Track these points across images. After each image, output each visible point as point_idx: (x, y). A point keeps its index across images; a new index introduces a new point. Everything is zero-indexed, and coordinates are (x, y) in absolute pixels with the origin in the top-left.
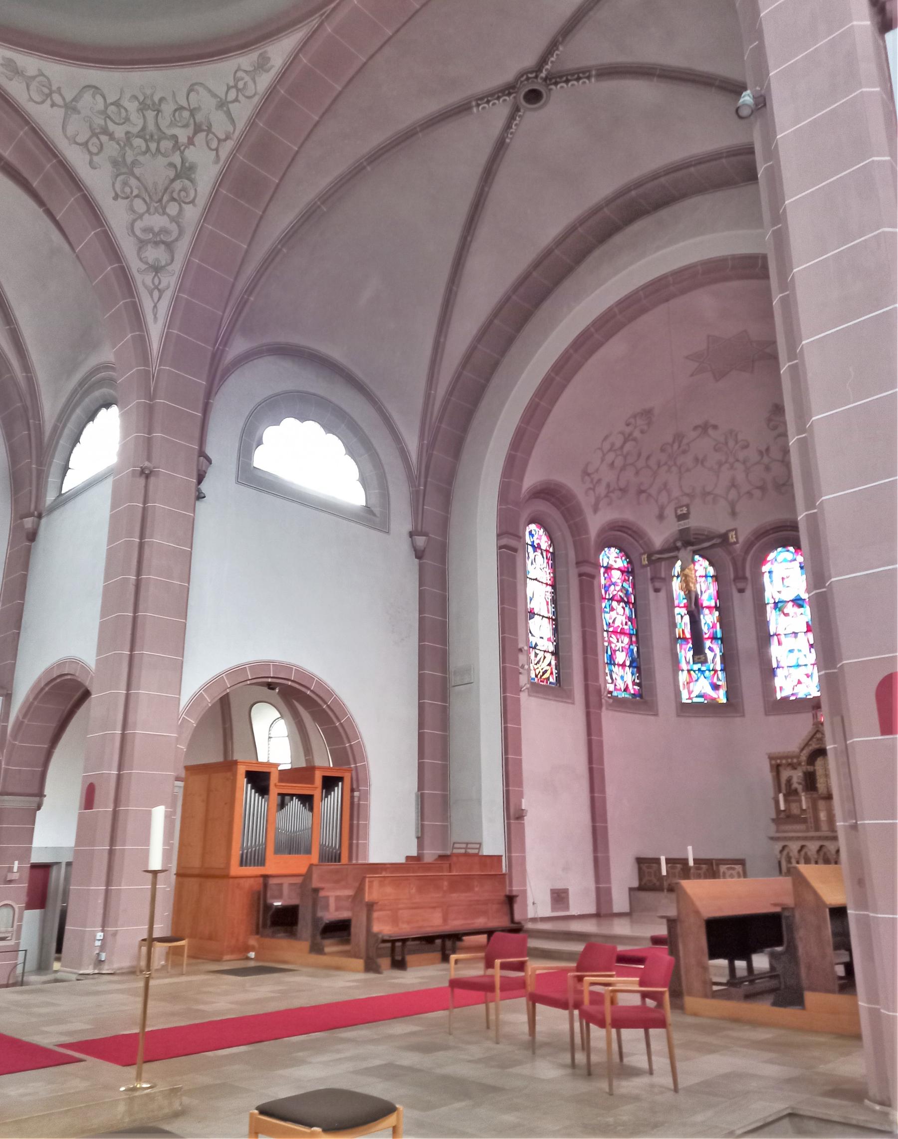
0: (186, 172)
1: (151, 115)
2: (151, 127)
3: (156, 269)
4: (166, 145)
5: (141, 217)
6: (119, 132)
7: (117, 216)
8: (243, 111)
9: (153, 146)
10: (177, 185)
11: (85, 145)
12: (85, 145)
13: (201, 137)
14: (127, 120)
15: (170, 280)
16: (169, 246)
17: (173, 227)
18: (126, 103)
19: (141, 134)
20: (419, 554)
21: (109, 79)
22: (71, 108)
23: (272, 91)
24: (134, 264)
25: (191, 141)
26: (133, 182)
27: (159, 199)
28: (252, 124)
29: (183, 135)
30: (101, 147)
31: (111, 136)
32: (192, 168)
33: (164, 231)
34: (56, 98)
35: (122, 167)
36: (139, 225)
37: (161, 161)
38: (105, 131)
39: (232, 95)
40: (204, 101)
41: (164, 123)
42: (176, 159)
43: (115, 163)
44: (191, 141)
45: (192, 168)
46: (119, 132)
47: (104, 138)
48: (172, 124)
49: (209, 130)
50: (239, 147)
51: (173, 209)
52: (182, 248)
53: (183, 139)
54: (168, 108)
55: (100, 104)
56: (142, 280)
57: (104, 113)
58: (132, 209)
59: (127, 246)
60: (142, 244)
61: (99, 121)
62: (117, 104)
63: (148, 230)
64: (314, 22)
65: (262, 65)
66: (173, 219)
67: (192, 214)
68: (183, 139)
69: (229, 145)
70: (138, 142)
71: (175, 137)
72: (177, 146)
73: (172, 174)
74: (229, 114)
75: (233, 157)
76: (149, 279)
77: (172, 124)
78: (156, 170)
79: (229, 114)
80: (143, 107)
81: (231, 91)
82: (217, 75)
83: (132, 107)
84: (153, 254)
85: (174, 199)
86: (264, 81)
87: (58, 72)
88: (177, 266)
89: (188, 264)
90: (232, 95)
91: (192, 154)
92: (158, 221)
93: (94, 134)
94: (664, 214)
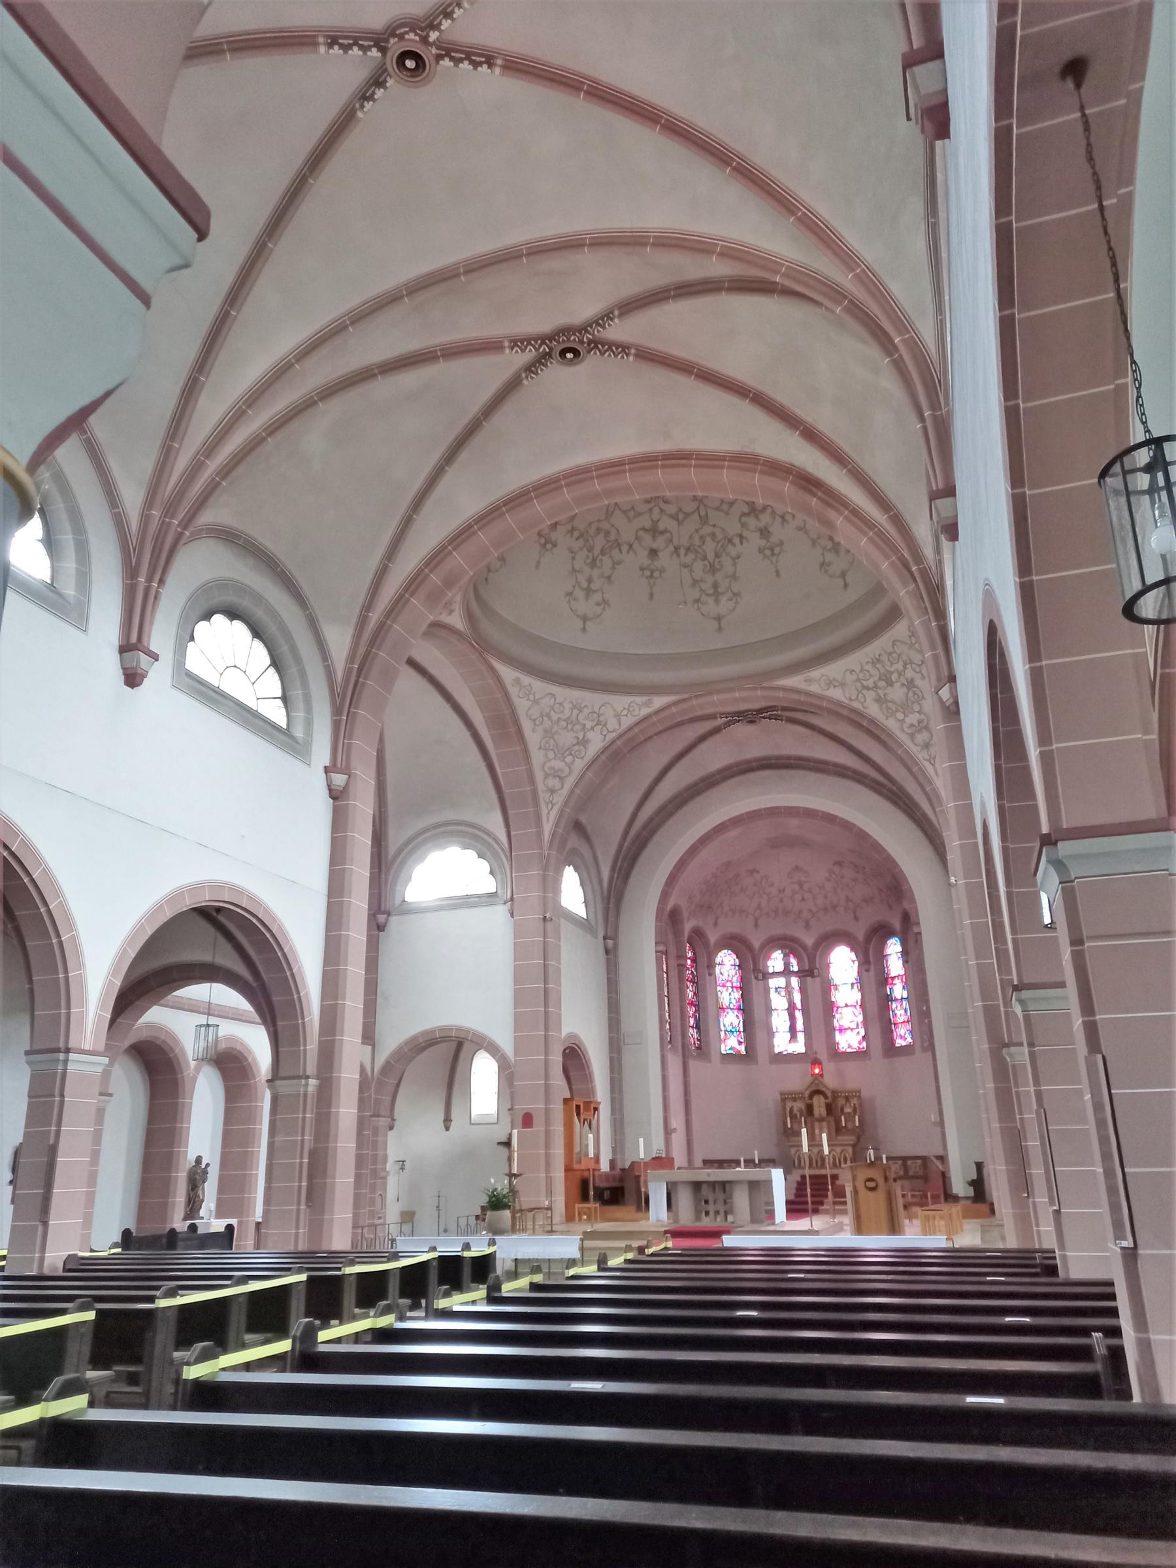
0: (584, 742)
1: (575, 712)
3: (552, 791)
4: (578, 727)
6: (555, 717)
7: (537, 758)
8: (627, 722)
9: (570, 727)
10: (576, 748)
11: (534, 720)
15: (559, 799)
16: (562, 779)
17: (567, 770)
18: (566, 705)
20: (607, 952)
21: (560, 692)
25: (592, 728)
26: (552, 742)
28: (630, 729)
29: (589, 725)
32: (588, 741)
33: (562, 771)
35: (549, 733)
37: (572, 734)
38: (548, 716)
39: (625, 712)
40: (608, 713)
41: (580, 717)
43: (546, 731)
44: (592, 728)
45: (588, 741)
46: (555, 717)
48: (587, 718)
49: (605, 725)
50: (620, 736)
51: (569, 759)
52: (570, 782)
53: (588, 726)
54: (586, 711)
56: (543, 796)
57: (552, 708)
58: (546, 756)
59: (539, 776)
60: (547, 776)
61: (547, 710)
62: (560, 704)
63: (551, 768)
66: (569, 766)
67: (579, 765)
68: (588, 726)
69: (614, 734)
70: (564, 724)
73: (575, 741)
75: (613, 742)
77: (587, 718)
78: (566, 738)
80: (574, 707)
82: (620, 702)
83: (567, 706)
84: (553, 782)
87: (538, 686)
89: (572, 791)
90: (625, 712)
91: (590, 735)
93: (542, 716)
94: (784, 772)
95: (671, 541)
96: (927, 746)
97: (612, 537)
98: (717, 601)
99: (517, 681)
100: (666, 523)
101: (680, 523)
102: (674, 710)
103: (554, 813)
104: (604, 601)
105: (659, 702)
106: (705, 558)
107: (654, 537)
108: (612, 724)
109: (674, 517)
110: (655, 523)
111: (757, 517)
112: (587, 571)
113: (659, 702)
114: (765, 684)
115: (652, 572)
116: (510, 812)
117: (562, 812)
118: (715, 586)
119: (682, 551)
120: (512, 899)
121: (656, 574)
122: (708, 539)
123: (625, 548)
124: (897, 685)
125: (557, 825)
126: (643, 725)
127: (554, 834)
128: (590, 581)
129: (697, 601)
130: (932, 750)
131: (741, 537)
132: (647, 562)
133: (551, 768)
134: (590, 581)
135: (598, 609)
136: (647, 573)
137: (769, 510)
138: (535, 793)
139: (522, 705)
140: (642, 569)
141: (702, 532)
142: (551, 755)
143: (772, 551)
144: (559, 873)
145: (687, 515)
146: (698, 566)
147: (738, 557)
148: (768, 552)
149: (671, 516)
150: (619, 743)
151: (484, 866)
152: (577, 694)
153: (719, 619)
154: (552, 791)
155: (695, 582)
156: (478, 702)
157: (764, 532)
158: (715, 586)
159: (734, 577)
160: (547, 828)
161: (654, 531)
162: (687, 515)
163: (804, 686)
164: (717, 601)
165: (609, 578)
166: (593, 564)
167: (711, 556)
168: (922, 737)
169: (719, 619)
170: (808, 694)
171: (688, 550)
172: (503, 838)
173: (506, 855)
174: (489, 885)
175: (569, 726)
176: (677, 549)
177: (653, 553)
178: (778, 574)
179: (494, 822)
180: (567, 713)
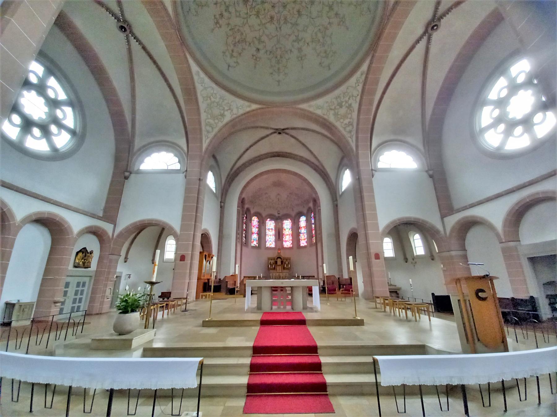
0: (223, 115)
1: (221, 100)
2: (220, 103)
3: (208, 132)
4: (221, 108)
5: (208, 119)
6: (213, 99)
7: (203, 116)
8: (241, 112)
12: (204, 97)
13: (229, 111)
14: (216, 98)
15: (211, 135)
16: (212, 128)
19: (217, 103)
22: (205, 88)
23: (248, 112)
24: (203, 128)
25: (227, 110)
26: (210, 111)
27: (214, 117)
28: (242, 115)
29: (226, 108)
30: (207, 100)
31: (210, 99)
34: (203, 85)
36: (207, 120)
42: (222, 112)
43: (208, 105)
44: (227, 110)
45: (225, 115)
47: (209, 99)
50: (236, 118)
51: (216, 121)
52: (216, 130)
54: (226, 102)
55: (212, 92)
56: (204, 133)
59: (203, 124)
60: (207, 125)
62: (215, 94)
64: (264, 106)
65: (249, 106)
67: (220, 125)
69: (235, 116)
70: (216, 104)
71: (224, 108)
72: (224, 109)
74: (238, 110)
76: (206, 133)
78: (216, 112)
79: (238, 110)
80: (220, 98)
81: (241, 107)
82: (240, 102)
83: (218, 96)
84: (209, 128)
85: (217, 119)
86: (248, 109)
87: (207, 80)
88: (214, 133)
91: (226, 113)
92: (211, 121)
93: (207, 97)
95: (265, 46)
96: (350, 132)
97: (243, 37)
98: (279, 76)
99: (198, 73)
100: (264, 38)
101: (270, 39)
102: (259, 111)
103: (208, 141)
104: (237, 62)
105: (254, 106)
106: (276, 57)
107: (259, 43)
108: (235, 111)
109: (267, 36)
110: (261, 36)
111: (298, 43)
112: (232, 47)
113: (254, 106)
114: (294, 106)
115: (256, 58)
116: (190, 136)
117: (211, 141)
118: (279, 69)
119: (268, 53)
120: (186, 171)
121: (258, 59)
122: (279, 50)
123: (248, 44)
124: (344, 107)
125: (209, 145)
126: (246, 115)
127: (207, 149)
128: (233, 51)
129: (272, 74)
130: (352, 134)
131: (291, 51)
132: (255, 53)
133: (208, 122)
134: (233, 51)
135: (235, 65)
136: (254, 58)
137: (303, 40)
138: (201, 129)
139: (199, 88)
140: (253, 56)
141: (277, 46)
142: (209, 116)
143: (301, 58)
144: (208, 172)
145: (273, 37)
146: (274, 61)
147: (289, 59)
148: (300, 59)
149: (266, 35)
150: (237, 120)
151: (176, 160)
152: (223, 92)
153: (279, 81)
154: (208, 132)
155: (272, 66)
156: (178, 78)
157: (300, 50)
158: (279, 69)
159: (286, 67)
160: (205, 146)
161: (260, 41)
162: (273, 37)
163: (308, 109)
164: (279, 76)
165: (240, 54)
166: (235, 45)
167: (279, 57)
168: (348, 129)
169: (279, 81)
170: (309, 111)
171: (271, 52)
172: (185, 149)
173: (185, 156)
174: (178, 166)
175: (219, 108)
176: (266, 52)
177: (258, 50)
178: (302, 67)
179: (182, 142)
180: (217, 100)
